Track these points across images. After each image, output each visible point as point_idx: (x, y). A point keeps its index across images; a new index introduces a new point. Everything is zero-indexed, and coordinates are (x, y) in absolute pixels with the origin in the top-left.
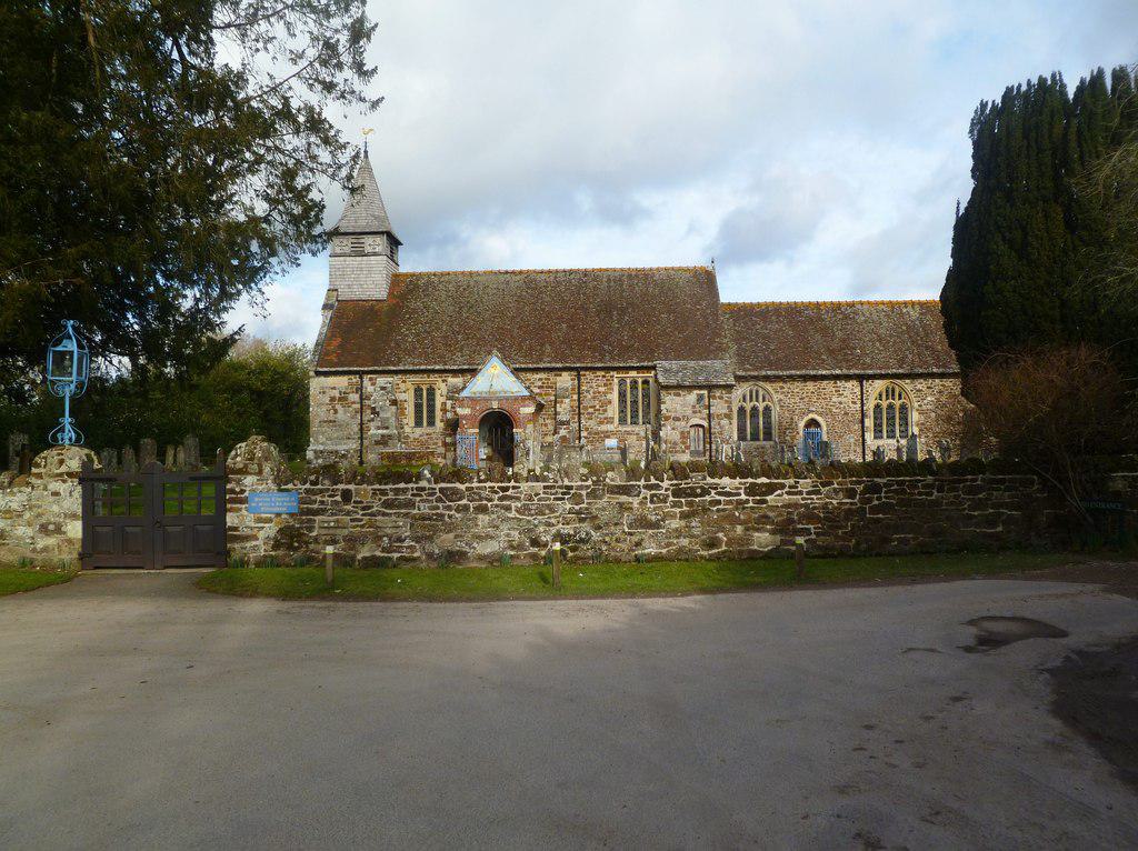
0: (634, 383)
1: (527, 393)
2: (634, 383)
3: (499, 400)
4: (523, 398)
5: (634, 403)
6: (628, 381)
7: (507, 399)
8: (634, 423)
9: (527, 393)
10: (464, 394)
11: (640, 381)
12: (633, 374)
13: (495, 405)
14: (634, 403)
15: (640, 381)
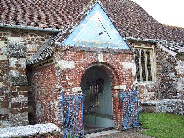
0: (143, 52)
1: (125, 47)
2: (143, 52)
3: (105, 52)
4: (124, 53)
5: (143, 66)
6: (140, 50)
7: (111, 52)
8: (144, 80)
9: (128, 48)
10: (68, 42)
11: (145, 51)
12: (143, 46)
13: (101, 58)
14: (143, 66)
15: (145, 51)
